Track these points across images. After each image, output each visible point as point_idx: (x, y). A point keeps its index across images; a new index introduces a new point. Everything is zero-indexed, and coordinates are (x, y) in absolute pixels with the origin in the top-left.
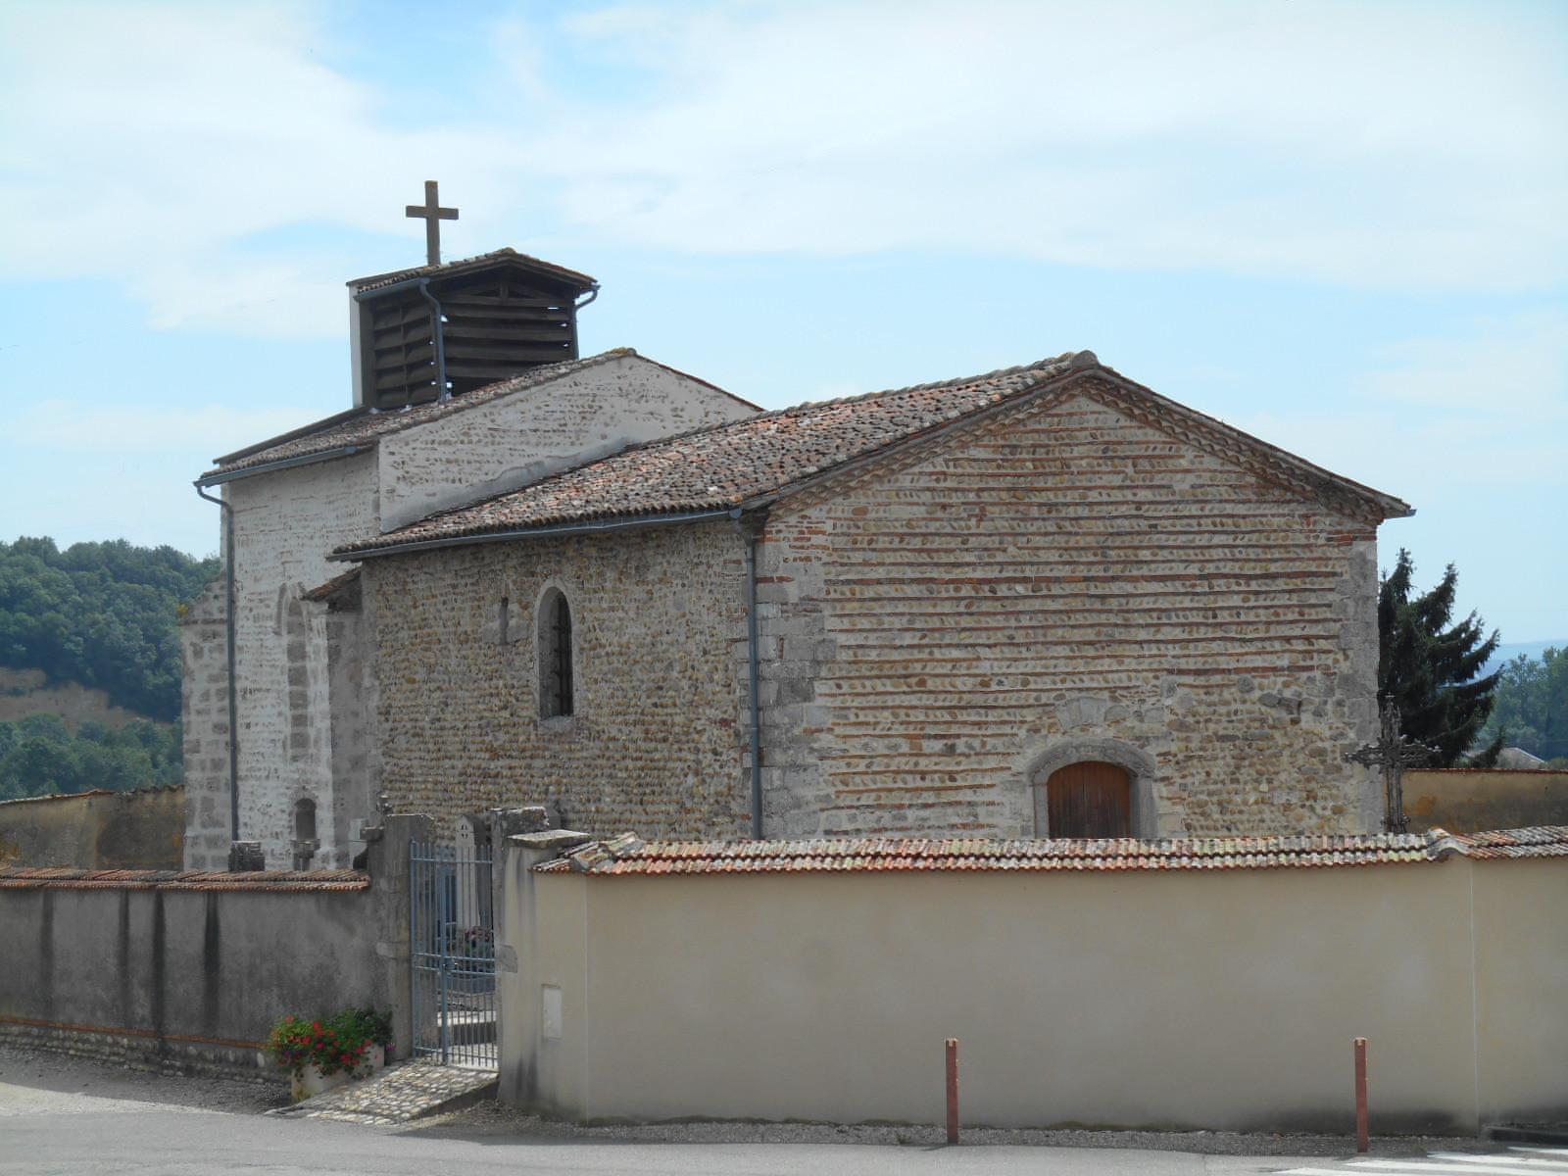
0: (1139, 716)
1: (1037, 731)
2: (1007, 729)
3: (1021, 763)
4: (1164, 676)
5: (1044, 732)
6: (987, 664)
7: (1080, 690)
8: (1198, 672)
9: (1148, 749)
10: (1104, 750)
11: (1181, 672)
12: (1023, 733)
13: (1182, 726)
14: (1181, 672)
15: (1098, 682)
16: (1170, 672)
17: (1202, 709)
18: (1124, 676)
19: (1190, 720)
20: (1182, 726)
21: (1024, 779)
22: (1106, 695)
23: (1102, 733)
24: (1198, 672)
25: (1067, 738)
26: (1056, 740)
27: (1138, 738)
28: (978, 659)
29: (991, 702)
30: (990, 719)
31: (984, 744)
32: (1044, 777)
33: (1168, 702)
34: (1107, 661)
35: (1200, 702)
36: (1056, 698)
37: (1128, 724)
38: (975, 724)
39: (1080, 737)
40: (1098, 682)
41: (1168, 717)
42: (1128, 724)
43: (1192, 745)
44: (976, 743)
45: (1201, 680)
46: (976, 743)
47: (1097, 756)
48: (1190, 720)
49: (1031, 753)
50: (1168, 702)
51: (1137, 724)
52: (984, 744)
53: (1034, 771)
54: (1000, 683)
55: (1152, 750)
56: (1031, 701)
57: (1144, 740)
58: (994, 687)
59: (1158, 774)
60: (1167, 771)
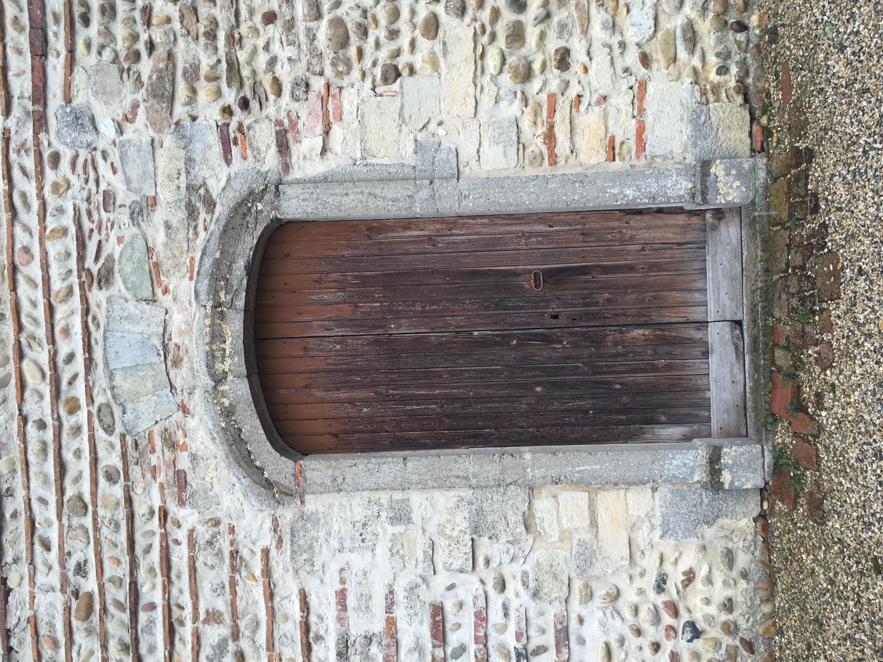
0: (142, 210)
1: (181, 480)
2: (180, 556)
3: (253, 521)
4: (56, 138)
5: (184, 462)
6: (43, 600)
7: (89, 363)
8: (40, 49)
9: (215, 187)
10: (218, 311)
11: (40, 94)
12: (188, 517)
13: (163, 93)
14: (40, 94)
15: (69, 313)
16: (40, 122)
17: (120, 31)
18: (54, 248)
19: (146, 66)
20: (163, 93)
21: (288, 514)
22: (97, 296)
23: (185, 311)
24: (40, 49)
25: (197, 402)
26: (201, 433)
27: (192, 213)
28: (34, 622)
29: (122, 595)
30: (157, 597)
31: (213, 617)
32: (278, 466)
33: (107, 128)
34: (23, 288)
35: (107, 33)
36: (109, 430)
37: (159, 238)
38: (171, 632)
39: (192, 372)
40: (69, 313)
41: (140, 130)
42: (159, 238)
43: (206, 61)
44: (213, 634)
45: (58, 43)
46: (213, 634)
47: (234, 327)
48: (146, 66)
49: (226, 491)
50: (107, 128)
51: (159, 216)
52: (213, 617)
53: (267, 487)
54: (81, 569)
55: (221, 178)
56: (118, 491)
57: (197, 199)
58: (90, 584)
59: (271, 161)
60: (264, 136)
